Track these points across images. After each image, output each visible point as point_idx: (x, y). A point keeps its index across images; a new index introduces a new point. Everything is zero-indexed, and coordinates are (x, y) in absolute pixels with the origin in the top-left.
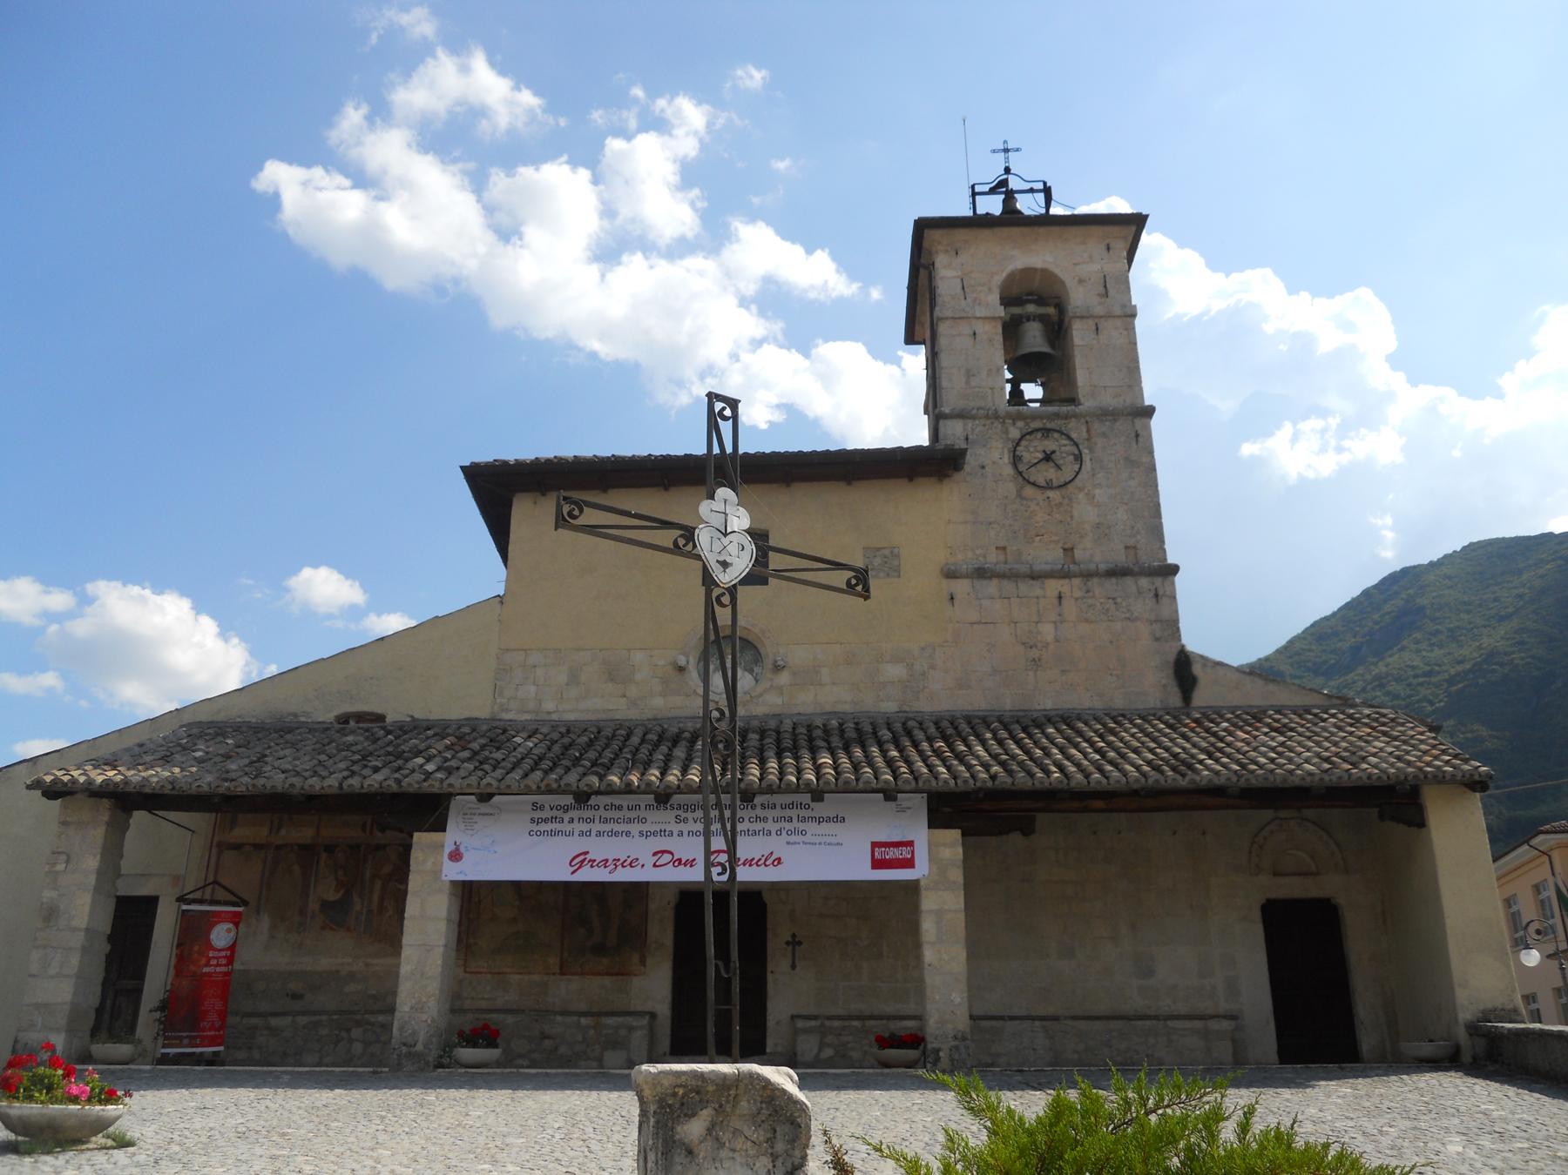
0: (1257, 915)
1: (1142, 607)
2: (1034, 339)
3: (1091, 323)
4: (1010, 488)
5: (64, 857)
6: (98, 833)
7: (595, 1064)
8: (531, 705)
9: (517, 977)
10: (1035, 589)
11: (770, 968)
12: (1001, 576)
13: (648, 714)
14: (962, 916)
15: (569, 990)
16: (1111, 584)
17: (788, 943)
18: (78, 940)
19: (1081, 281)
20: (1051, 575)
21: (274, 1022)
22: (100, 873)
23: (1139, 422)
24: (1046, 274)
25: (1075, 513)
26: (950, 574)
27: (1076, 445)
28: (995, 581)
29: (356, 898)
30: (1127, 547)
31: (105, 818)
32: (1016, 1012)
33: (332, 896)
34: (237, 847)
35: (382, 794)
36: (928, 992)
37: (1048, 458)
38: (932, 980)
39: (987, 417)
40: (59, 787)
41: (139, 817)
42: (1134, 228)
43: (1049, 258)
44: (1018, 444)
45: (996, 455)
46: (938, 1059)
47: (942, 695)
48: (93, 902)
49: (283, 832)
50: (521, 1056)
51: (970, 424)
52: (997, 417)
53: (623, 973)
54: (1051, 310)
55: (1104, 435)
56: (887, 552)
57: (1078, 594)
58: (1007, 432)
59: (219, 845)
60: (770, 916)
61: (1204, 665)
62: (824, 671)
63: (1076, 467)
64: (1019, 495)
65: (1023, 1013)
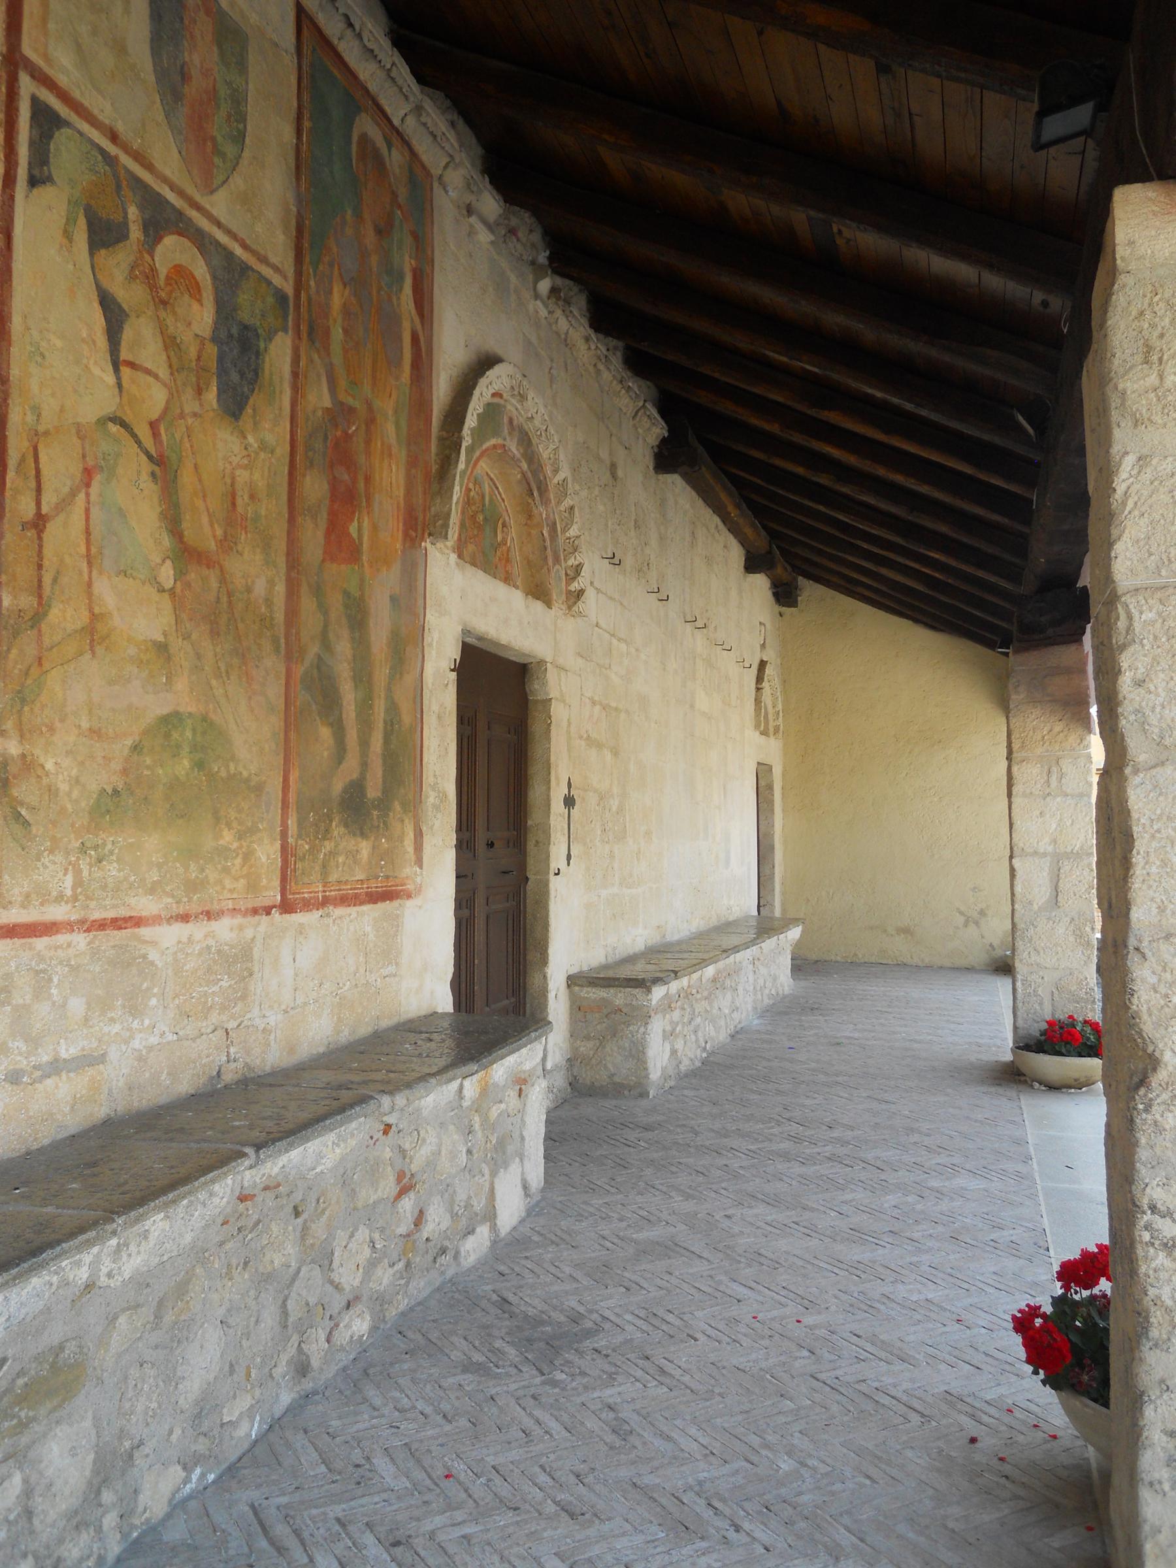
9: (170, 935)
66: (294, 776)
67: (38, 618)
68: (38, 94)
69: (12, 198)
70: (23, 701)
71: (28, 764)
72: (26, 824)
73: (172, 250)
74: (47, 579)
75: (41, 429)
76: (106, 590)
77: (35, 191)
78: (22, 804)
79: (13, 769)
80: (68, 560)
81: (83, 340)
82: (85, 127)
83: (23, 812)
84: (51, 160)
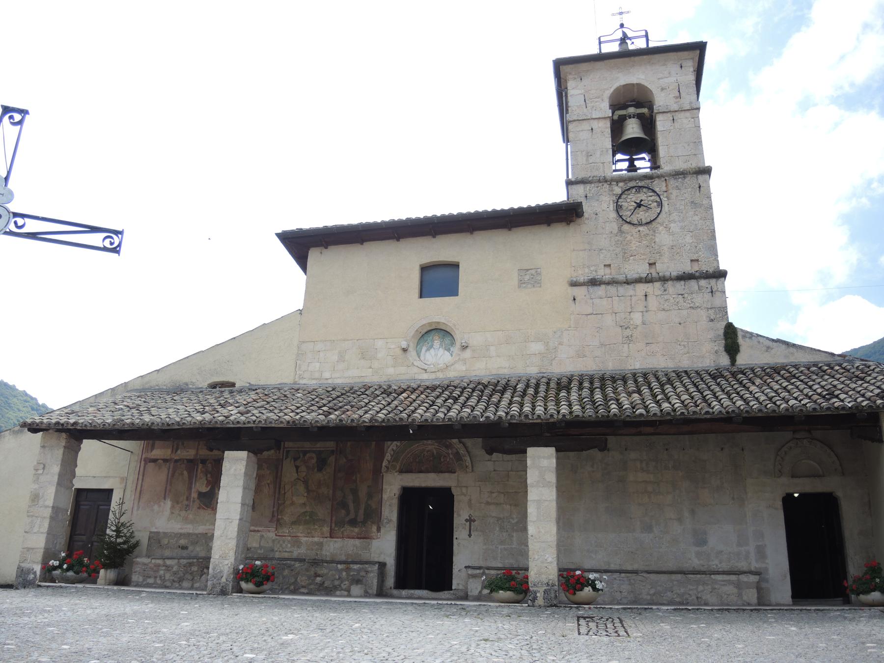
0: (779, 504)
1: (701, 299)
2: (633, 130)
3: (669, 115)
4: (614, 226)
5: (42, 466)
6: (59, 453)
7: (346, 593)
8: (317, 375)
9: (305, 539)
10: (629, 290)
11: (455, 537)
12: (608, 283)
13: (384, 379)
14: (554, 504)
15: (334, 547)
16: (680, 286)
17: (467, 520)
18: (48, 512)
19: (662, 89)
20: (639, 280)
21: (168, 562)
22: (60, 475)
23: (701, 178)
24: (640, 87)
25: (657, 240)
26: (574, 284)
27: (659, 196)
28: (603, 286)
30: (692, 261)
31: (64, 444)
32: (613, 567)
33: (204, 489)
34: (154, 461)
35: (202, 428)
36: (530, 553)
37: (639, 205)
38: (533, 545)
39: (599, 181)
40: (35, 427)
41: (89, 446)
42: (698, 52)
43: (643, 77)
44: (620, 198)
45: (605, 206)
46: (535, 598)
47: (566, 364)
48: (57, 491)
49: (179, 452)
50: (303, 587)
51: (588, 186)
52: (606, 181)
53: (365, 537)
54: (645, 110)
55: (678, 188)
56: (533, 272)
57: (660, 293)
58: (612, 191)
59: (145, 460)
60: (456, 503)
61: (744, 337)
62: (492, 348)
63: (658, 210)
64: (620, 231)
65: (617, 568)
66: (334, 518)
73: (308, 455)
76: (294, 499)
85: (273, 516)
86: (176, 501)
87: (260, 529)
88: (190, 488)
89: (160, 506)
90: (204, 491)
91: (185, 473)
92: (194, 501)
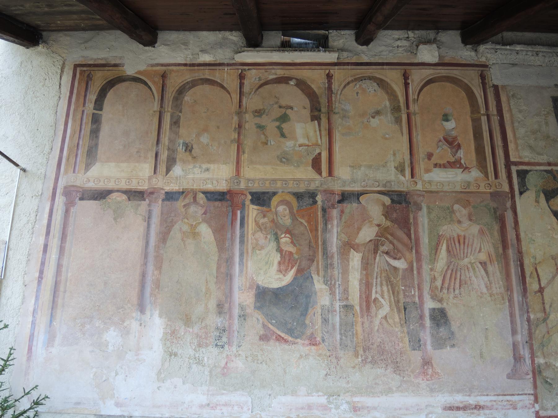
29: (319, 285)
33: (275, 279)
34: (100, 195)
49: (177, 170)
59: (68, 192)
67: (545, 320)
68: (518, 169)
69: (515, 201)
70: (543, 346)
71: (548, 365)
72: (550, 384)
74: (547, 307)
75: (537, 262)
77: (522, 196)
78: (548, 378)
79: (542, 367)
80: (555, 298)
81: (549, 230)
82: (538, 168)
83: (548, 380)
84: (527, 184)
85: (518, 358)
86: (182, 316)
87: (482, 400)
88: (225, 277)
89: (126, 332)
90: (275, 285)
91: (205, 230)
92: (243, 317)
